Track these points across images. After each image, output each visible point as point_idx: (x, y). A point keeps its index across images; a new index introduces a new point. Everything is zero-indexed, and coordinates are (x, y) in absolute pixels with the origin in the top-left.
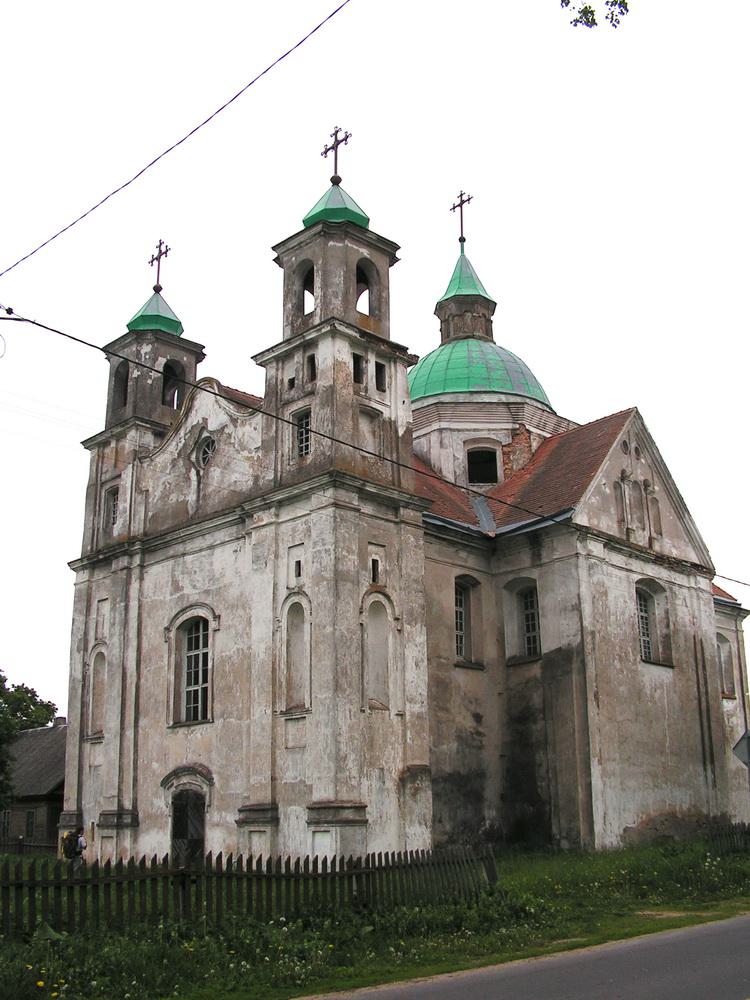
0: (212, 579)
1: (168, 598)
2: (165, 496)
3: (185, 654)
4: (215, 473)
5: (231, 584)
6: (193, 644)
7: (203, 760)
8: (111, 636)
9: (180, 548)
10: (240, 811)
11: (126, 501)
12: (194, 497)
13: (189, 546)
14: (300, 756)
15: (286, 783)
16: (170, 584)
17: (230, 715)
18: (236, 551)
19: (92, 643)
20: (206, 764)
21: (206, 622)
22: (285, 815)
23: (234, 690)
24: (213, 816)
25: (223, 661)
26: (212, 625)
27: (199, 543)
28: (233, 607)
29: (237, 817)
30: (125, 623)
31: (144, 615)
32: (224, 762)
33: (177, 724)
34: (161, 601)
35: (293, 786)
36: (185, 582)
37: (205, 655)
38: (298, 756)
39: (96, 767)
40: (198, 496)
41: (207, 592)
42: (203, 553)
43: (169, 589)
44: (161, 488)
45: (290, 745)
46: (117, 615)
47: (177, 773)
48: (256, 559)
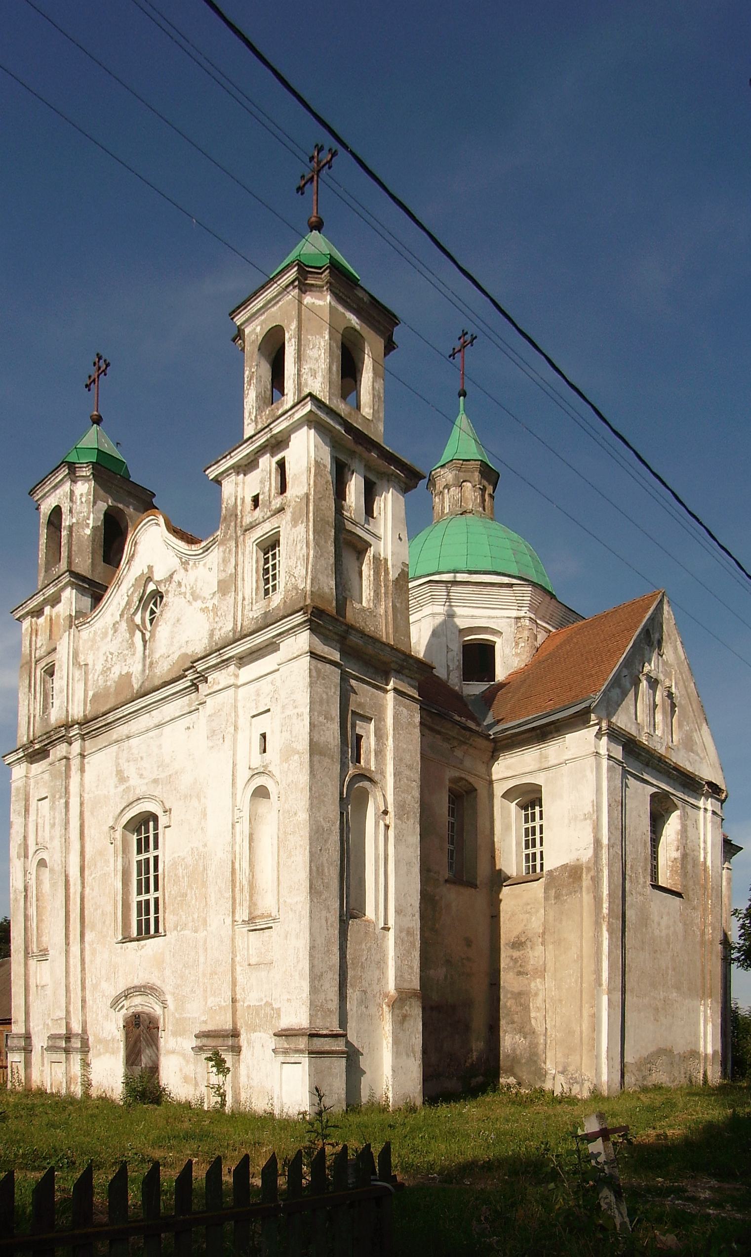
2: (106, 671)
3: (135, 858)
4: (163, 630)
6: (143, 846)
8: (52, 838)
10: (197, 1036)
11: (61, 678)
15: (249, 1006)
16: (114, 775)
18: (189, 728)
19: (32, 849)
21: (155, 818)
22: (249, 1043)
24: (167, 1041)
26: (162, 821)
27: (144, 721)
28: (186, 797)
29: (194, 1043)
31: (87, 815)
33: (127, 939)
35: (257, 1009)
36: (130, 771)
37: (156, 858)
38: (263, 974)
40: (144, 665)
41: (156, 781)
42: (151, 734)
43: (113, 780)
44: (102, 660)
45: (253, 961)
46: (57, 814)
48: (212, 733)
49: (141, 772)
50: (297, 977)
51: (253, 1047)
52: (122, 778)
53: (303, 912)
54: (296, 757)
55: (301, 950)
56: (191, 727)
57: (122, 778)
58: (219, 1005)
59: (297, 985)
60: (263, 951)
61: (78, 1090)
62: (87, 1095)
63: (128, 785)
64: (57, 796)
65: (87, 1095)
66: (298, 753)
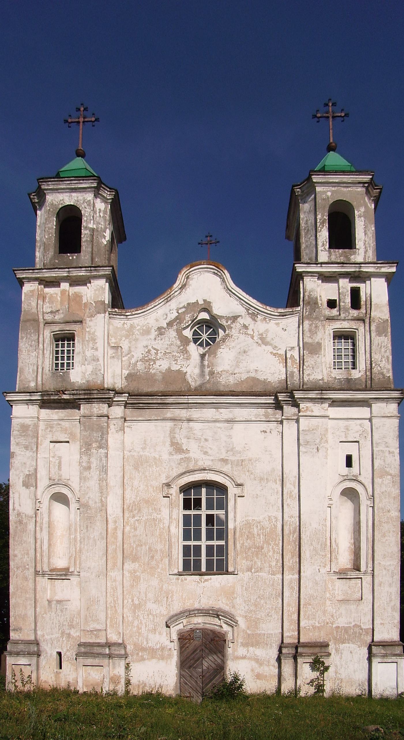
0: (231, 450)
1: (165, 456)
5: (258, 460)
7: (222, 604)
9: (183, 413)
12: (197, 371)
13: (195, 413)
14: (355, 606)
15: (338, 627)
17: (261, 569)
19: (43, 482)
20: (227, 608)
22: (337, 650)
23: (265, 550)
25: (248, 525)
26: (232, 491)
27: (209, 413)
28: (261, 479)
30: (104, 469)
32: (252, 608)
34: (155, 458)
38: (353, 607)
39: (59, 602)
41: (225, 461)
42: (218, 424)
43: (167, 448)
45: (340, 598)
47: (189, 613)
49: (205, 450)
50: (390, 610)
51: (341, 653)
52: (177, 448)
53: (395, 571)
54: (389, 477)
55: (393, 594)
56: (268, 431)
57: (177, 448)
58: (313, 626)
59: (389, 615)
60: (349, 592)
61: (121, 689)
62: (127, 692)
63: (187, 456)
64: (94, 445)
65: (127, 692)
66: (391, 475)
